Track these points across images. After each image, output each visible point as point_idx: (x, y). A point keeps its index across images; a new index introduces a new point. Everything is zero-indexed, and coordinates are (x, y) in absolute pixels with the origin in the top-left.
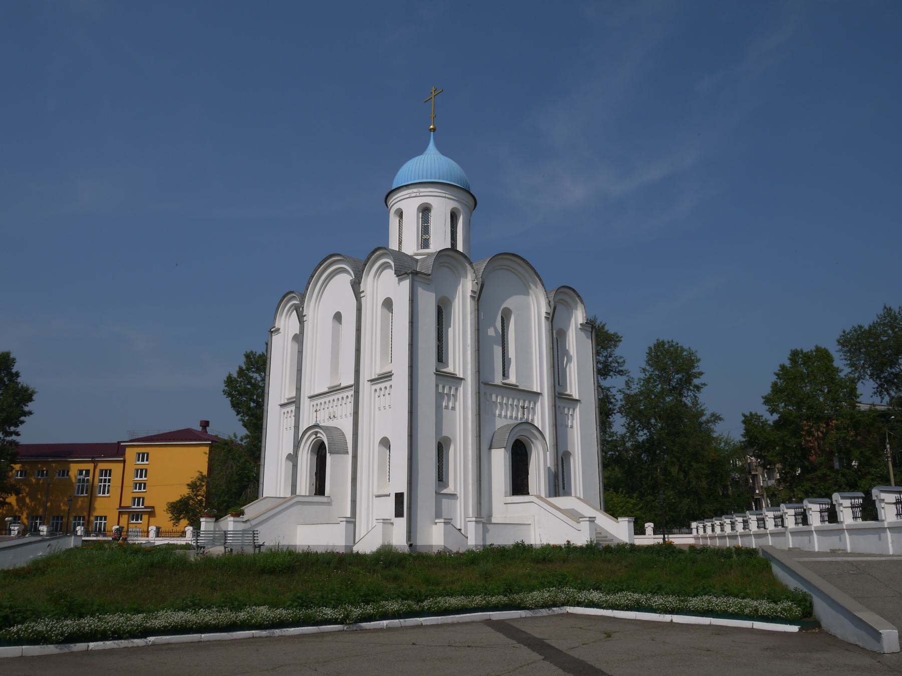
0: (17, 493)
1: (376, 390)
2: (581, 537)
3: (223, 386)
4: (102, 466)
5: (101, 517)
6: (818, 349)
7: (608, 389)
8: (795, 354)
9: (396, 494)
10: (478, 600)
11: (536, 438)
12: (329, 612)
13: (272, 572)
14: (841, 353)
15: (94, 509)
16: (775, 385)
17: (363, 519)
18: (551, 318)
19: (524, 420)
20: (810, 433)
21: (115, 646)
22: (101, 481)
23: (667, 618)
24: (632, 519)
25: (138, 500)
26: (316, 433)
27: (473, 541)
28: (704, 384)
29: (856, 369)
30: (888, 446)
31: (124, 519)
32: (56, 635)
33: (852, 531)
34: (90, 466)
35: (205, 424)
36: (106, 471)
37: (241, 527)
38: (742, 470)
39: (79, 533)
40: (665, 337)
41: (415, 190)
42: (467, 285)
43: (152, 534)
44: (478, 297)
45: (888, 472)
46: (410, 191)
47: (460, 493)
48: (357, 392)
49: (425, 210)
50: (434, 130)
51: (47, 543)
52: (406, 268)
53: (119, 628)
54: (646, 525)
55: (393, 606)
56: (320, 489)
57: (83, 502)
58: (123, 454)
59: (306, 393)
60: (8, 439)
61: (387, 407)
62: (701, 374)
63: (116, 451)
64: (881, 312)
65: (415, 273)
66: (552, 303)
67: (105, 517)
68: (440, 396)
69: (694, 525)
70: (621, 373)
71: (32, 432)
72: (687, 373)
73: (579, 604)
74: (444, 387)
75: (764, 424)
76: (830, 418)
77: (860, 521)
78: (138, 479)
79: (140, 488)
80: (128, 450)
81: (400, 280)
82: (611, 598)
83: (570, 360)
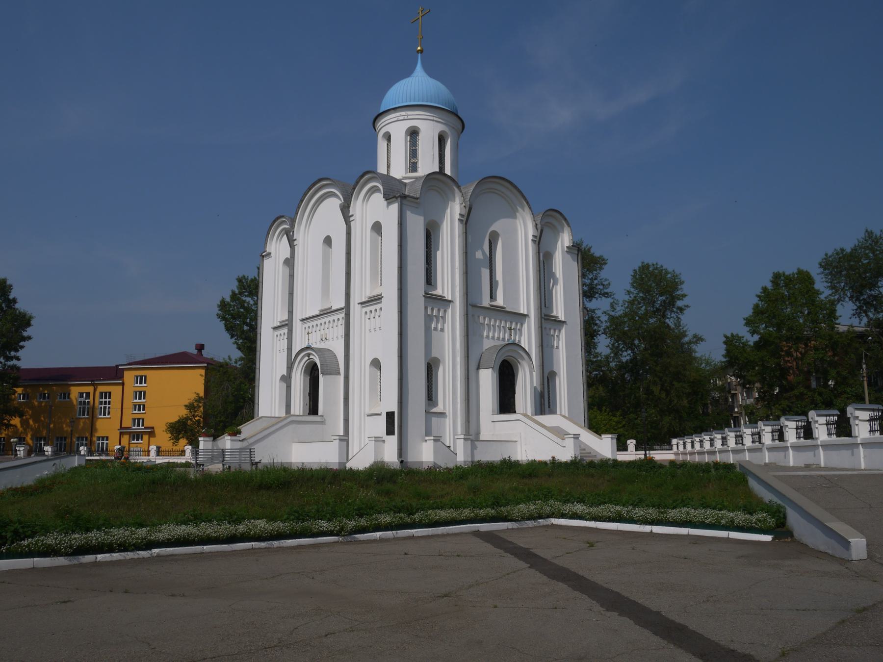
0: (21, 415)
1: (366, 313)
2: (566, 454)
3: (216, 310)
4: (101, 389)
5: (103, 438)
6: (800, 272)
7: (593, 311)
8: (777, 277)
9: (387, 413)
10: (466, 513)
11: (523, 359)
12: (324, 525)
13: (268, 487)
14: (822, 276)
15: (96, 430)
16: (756, 306)
17: (356, 437)
18: (538, 241)
19: (511, 341)
20: (789, 354)
21: (122, 558)
22: (101, 403)
23: (647, 528)
24: (615, 436)
25: (138, 421)
26: (309, 355)
27: (461, 457)
28: (687, 306)
29: (837, 291)
30: (864, 366)
31: (125, 439)
32: (65, 548)
33: (826, 446)
34: (90, 389)
36: (106, 393)
37: (238, 445)
38: (722, 389)
39: (82, 453)
40: (650, 260)
41: (403, 113)
42: (455, 209)
43: (153, 453)
44: (466, 220)
45: (863, 392)
46: (398, 114)
47: (449, 411)
48: (348, 315)
49: (413, 133)
50: (421, 51)
51: (52, 463)
52: (394, 192)
53: (125, 541)
54: (629, 442)
55: (386, 519)
56: (313, 409)
57: (84, 423)
59: (298, 315)
60: (9, 363)
61: (378, 329)
62: (684, 296)
63: (115, 374)
64: (861, 235)
65: (404, 197)
66: (539, 226)
67: (107, 440)
68: (429, 319)
69: (674, 441)
70: (606, 295)
71: (32, 356)
72: (671, 295)
73: (563, 516)
74: (433, 309)
75: (745, 344)
76: (809, 339)
77: (834, 437)
78: (137, 400)
79: (139, 410)
80: (126, 373)
81: (389, 204)
82: (594, 510)
83: (556, 282)
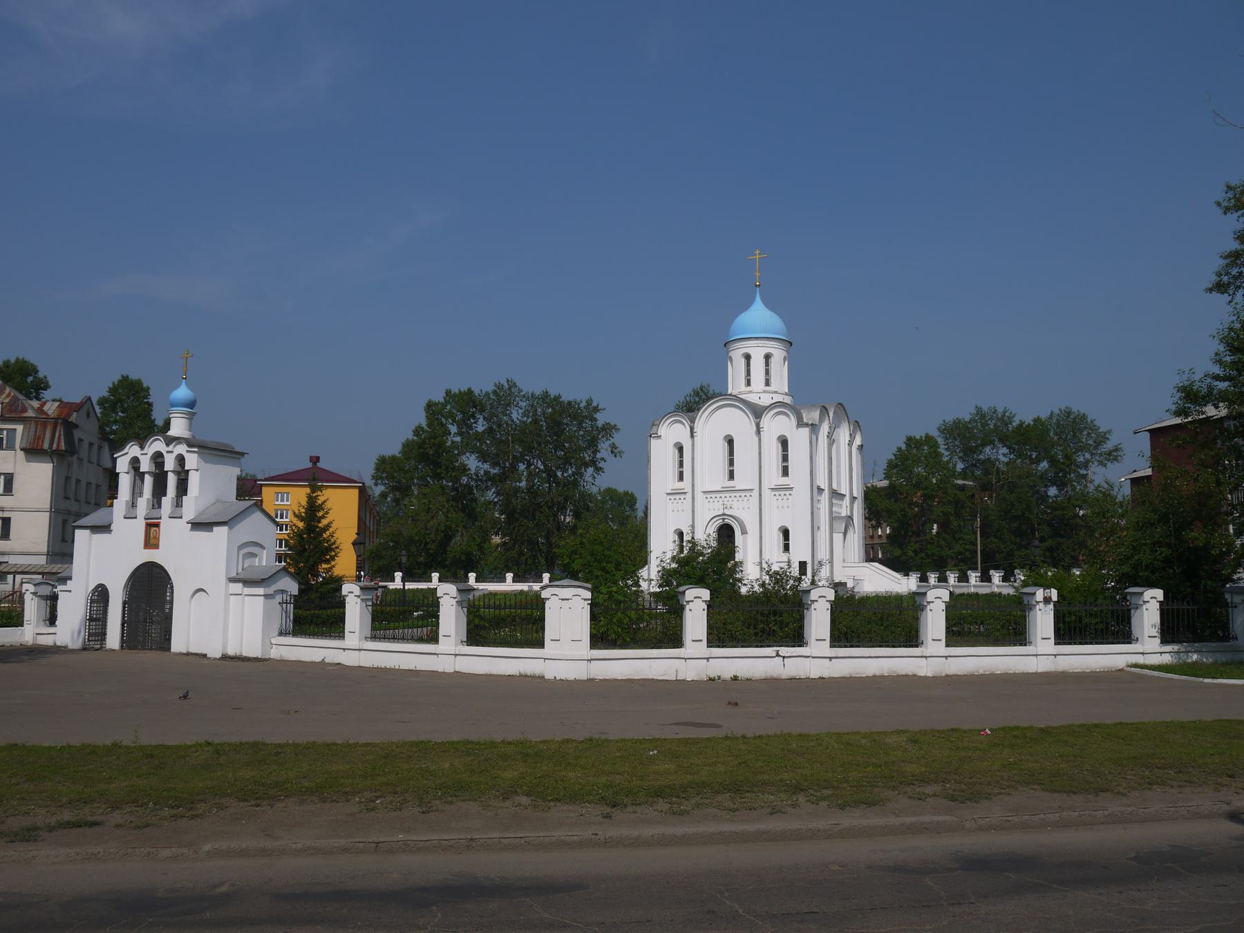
8: (910, 440)
35: (315, 460)
44: (830, 436)
58: (260, 494)
